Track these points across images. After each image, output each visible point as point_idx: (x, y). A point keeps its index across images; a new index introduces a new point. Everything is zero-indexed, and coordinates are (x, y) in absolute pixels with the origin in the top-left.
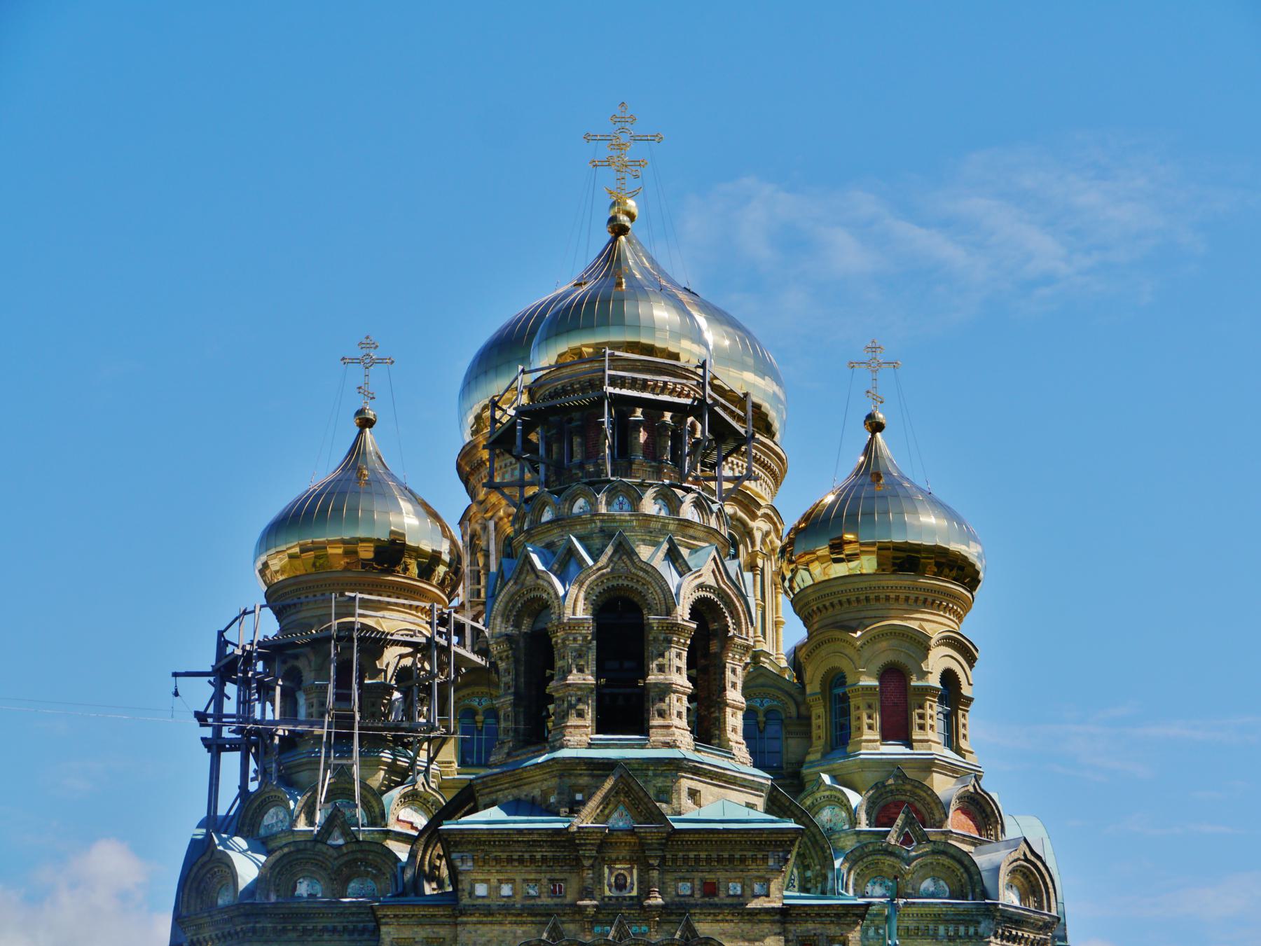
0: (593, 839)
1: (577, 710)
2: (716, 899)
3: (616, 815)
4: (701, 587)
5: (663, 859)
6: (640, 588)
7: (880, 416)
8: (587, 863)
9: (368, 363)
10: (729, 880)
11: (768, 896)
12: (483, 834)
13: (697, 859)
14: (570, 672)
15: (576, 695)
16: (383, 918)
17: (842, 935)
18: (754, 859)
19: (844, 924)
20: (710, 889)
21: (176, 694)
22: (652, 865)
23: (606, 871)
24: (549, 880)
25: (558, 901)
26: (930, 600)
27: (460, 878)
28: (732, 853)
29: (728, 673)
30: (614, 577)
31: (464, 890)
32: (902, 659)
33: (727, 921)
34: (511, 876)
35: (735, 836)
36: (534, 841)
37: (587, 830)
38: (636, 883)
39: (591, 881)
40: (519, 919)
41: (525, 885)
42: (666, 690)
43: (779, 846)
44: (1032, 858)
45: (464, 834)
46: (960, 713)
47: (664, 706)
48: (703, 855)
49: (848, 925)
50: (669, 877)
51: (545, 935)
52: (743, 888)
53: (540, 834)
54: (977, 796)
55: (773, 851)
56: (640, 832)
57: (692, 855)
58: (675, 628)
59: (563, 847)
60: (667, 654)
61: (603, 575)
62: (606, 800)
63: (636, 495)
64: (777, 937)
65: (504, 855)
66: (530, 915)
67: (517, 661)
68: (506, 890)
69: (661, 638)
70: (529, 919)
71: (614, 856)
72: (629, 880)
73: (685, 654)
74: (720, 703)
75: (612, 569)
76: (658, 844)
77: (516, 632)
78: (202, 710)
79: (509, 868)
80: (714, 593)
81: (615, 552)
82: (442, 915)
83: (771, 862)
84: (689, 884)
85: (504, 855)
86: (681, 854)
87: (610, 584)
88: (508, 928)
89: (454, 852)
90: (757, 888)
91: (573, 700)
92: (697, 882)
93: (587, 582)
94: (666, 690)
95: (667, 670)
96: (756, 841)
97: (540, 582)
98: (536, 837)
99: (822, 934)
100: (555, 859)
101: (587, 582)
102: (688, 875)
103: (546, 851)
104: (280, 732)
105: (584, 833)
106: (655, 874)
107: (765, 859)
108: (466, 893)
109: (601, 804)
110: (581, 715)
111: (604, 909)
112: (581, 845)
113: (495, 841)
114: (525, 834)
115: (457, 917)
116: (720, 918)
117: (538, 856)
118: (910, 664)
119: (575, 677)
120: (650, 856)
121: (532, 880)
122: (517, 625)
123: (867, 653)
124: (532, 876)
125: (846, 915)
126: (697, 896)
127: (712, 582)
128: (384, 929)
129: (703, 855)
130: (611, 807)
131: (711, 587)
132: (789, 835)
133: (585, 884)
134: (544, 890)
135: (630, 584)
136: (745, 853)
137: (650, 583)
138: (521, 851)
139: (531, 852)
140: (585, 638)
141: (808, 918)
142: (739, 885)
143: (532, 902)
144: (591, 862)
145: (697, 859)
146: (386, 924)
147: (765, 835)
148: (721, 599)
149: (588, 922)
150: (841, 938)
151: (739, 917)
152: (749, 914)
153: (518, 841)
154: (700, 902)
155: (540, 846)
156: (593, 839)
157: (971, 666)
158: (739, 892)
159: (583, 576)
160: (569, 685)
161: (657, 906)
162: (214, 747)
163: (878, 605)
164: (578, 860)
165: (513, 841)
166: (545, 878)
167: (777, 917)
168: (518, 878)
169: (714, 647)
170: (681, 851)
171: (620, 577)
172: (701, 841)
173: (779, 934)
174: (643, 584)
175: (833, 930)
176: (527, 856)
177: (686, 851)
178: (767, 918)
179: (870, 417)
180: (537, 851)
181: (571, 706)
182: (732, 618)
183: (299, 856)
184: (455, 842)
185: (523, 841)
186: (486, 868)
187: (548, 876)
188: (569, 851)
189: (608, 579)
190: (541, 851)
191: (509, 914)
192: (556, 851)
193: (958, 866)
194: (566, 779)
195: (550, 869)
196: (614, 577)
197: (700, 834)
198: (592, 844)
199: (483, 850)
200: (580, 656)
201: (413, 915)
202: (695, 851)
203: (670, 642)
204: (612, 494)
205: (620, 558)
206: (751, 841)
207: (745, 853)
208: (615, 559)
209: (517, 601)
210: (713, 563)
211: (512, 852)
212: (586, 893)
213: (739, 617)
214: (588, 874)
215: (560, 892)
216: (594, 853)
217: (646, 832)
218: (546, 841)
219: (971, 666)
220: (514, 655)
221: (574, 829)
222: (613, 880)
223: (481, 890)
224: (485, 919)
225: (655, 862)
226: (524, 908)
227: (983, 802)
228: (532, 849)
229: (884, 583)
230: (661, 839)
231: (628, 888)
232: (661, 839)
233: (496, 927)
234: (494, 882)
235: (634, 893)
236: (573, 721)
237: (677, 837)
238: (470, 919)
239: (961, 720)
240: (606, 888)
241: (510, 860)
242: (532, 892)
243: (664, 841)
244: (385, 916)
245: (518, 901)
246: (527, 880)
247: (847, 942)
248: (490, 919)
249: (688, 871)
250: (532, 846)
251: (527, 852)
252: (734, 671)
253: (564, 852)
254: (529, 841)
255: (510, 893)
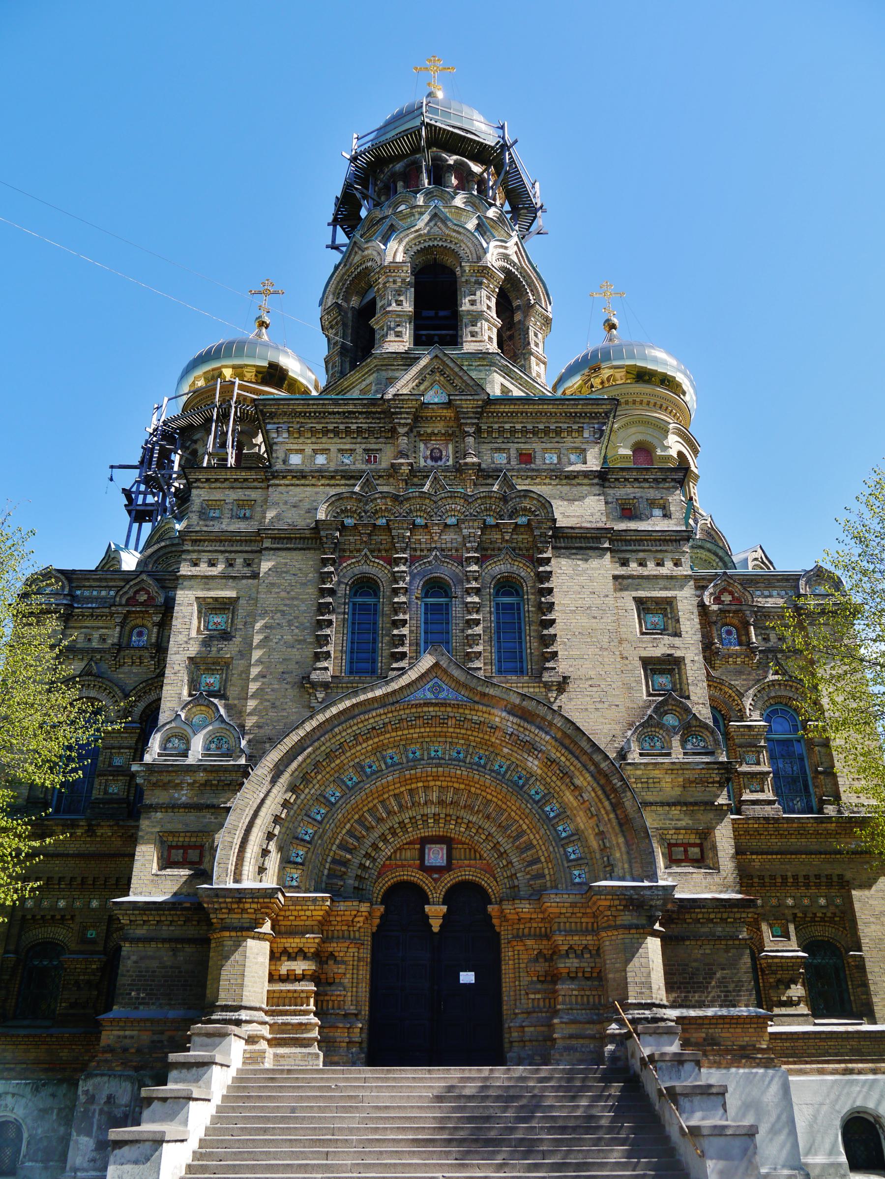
0: (409, 408)
1: (396, 332)
2: (533, 466)
3: (431, 393)
4: (506, 257)
5: (479, 430)
6: (453, 247)
7: (615, 320)
8: (402, 430)
9: (266, 293)
10: (545, 450)
11: (585, 463)
12: (299, 404)
13: (513, 431)
14: (391, 305)
15: (395, 322)
16: (195, 482)
17: (662, 498)
18: (570, 432)
19: (663, 488)
20: (526, 458)
21: (111, 479)
22: (466, 432)
23: (422, 446)
24: (364, 450)
25: (373, 467)
26: (664, 406)
27: (275, 447)
28: (547, 425)
29: (531, 334)
30: (430, 239)
31: (278, 458)
32: (649, 439)
33: (545, 484)
34: (326, 446)
35: (550, 407)
36: (350, 412)
37: (402, 397)
38: (451, 456)
39: (405, 446)
40: (332, 482)
41: (340, 455)
42: (477, 317)
43: (594, 418)
44: (767, 562)
45: (279, 405)
46: (691, 484)
47: (476, 329)
48: (519, 426)
49: (668, 489)
50: (484, 448)
51: (357, 489)
52: (559, 458)
53: (355, 405)
54: (713, 533)
55: (588, 423)
56: (456, 400)
57: (507, 426)
58: (485, 271)
59: (378, 418)
60: (478, 293)
61: (420, 235)
62: (421, 377)
63: (449, 197)
64: (597, 497)
65: (319, 426)
66: (343, 477)
67: (345, 325)
68: (321, 460)
69: (473, 279)
70: (343, 482)
71: (429, 431)
72: (444, 453)
73: (494, 300)
74: (525, 354)
75: (429, 232)
76: (473, 412)
77: (345, 305)
78: (128, 488)
79: (324, 440)
80: (517, 270)
81: (430, 220)
82: (255, 480)
83: (586, 435)
84: (505, 455)
85: (319, 426)
86: (496, 426)
87: (426, 244)
88: (321, 489)
89: (269, 423)
90: (573, 457)
91: (392, 325)
92: (513, 452)
93: (407, 240)
94: (477, 317)
95: (478, 304)
96: (571, 413)
97: (366, 253)
98: (351, 408)
99: (641, 497)
100: (370, 431)
101: (407, 240)
102: (503, 446)
103: (361, 423)
104: (176, 484)
105: (399, 400)
106: (470, 440)
107: (580, 431)
108: (280, 461)
109: (416, 379)
110: (398, 335)
111: (420, 472)
112: (396, 413)
113: (310, 413)
114: (340, 405)
115: (269, 480)
116: (538, 481)
117: (354, 427)
118: (655, 442)
119: (394, 307)
120: (466, 424)
121: (346, 450)
122: (347, 299)
123: (622, 434)
124: (347, 447)
125: (664, 480)
126: (514, 462)
127: (514, 258)
128: (194, 492)
129: (519, 426)
130: (426, 384)
131: (515, 264)
132: (604, 407)
133: (400, 448)
134: (358, 458)
135: (445, 244)
136: (560, 425)
137: (462, 241)
138: (336, 423)
139: (347, 423)
140: (403, 281)
141: (627, 483)
142: (555, 455)
143: (347, 467)
144: (406, 429)
145: (513, 431)
146: (198, 487)
147: (580, 407)
148: (524, 277)
149: (402, 480)
150: (661, 502)
151: (557, 480)
152: (567, 477)
153: (334, 413)
154: (517, 467)
155: (356, 418)
156: (409, 408)
157: (696, 457)
158: (555, 462)
159: (402, 235)
160: (389, 312)
161: (473, 464)
162: (134, 513)
163: (627, 407)
164: (393, 431)
165: (330, 413)
166: (359, 448)
167: (596, 481)
168: (333, 448)
169: (518, 317)
170: (496, 423)
171: (435, 239)
172: (517, 413)
173: (599, 495)
174: (456, 244)
175: (652, 494)
176: (342, 427)
177: (501, 423)
178: (586, 481)
179: (608, 320)
180: (352, 423)
181: (390, 328)
182: (533, 295)
183: (174, 549)
184: (271, 413)
185: (338, 413)
186: (301, 441)
187: (364, 446)
188: (385, 423)
189: (425, 241)
190: (356, 423)
191: (323, 477)
192: (371, 423)
193: (714, 557)
194: (384, 373)
195: (365, 440)
196: (430, 239)
197: (515, 404)
198: (407, 413)
199: (298, 422)
200: (399, 295)
201: (226, 480)
202: (510, 423)
203: (481, 283)
204: (429, 195)
205: (435, 225)
206: (566, 413)
207: (560, 425)
208: (432, 224)
209: (346, 280)
210: (516, 248)
211: (327, 423)
212: (402, 454)
213: (539, 295)
214: (403, 441)
215: (375, 462)
216: (409, 421)
217: (461, 400)
218: (360, 413)
219: (696, 457)
220: (342, 319)
221: (388, 396)
222: (428, 453)
223: (295, 460)
224: (298, 482)
225: (471, 430)
226: (336, 471)
227: (717, 538)
228: (347, 420)
229: (631, 391)
230: (477, 407)
231: (444, 460)
232: (477, 407)
233: (308, 489)
234: (308, 450)
235: (450, 463)
236: (391, 338)
237: (492, 408)
238: (282, 482)
239: (692, 490)
240: (422, 460)
241: (325, 432)
242: (347, 461)
243: (479, 410)
244: (198, 480)
245: (332, 467)
246: (342, 450)
247: (667, 505)
248: (302, 482)
249: (503, 442)
250: (347, 417)
251: (342, 423)
252: (536, 335)
253: (379, 423)
254: (344, 413)
255: (325, 462)
